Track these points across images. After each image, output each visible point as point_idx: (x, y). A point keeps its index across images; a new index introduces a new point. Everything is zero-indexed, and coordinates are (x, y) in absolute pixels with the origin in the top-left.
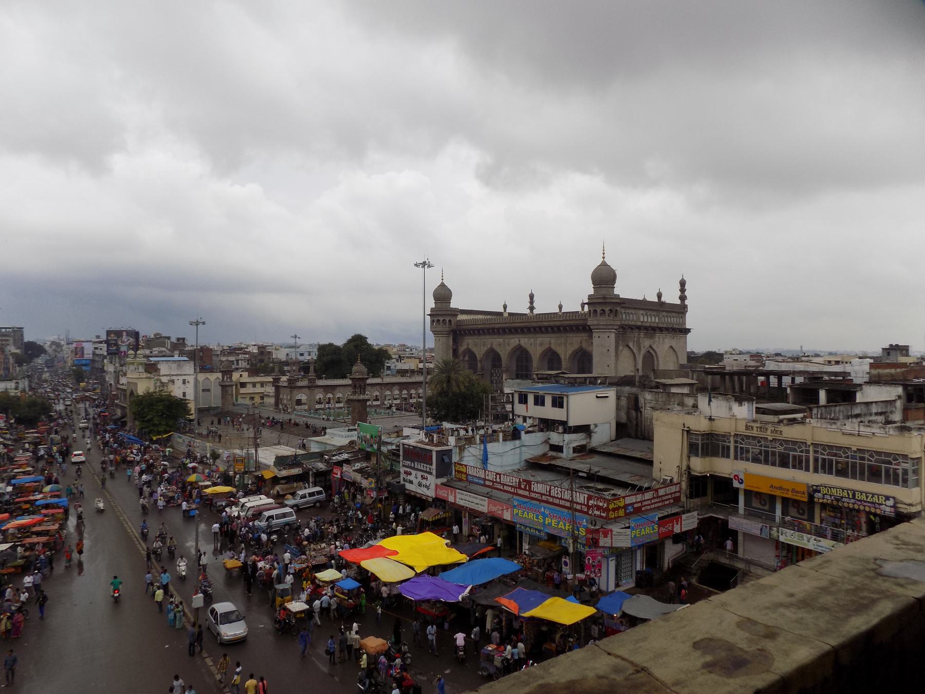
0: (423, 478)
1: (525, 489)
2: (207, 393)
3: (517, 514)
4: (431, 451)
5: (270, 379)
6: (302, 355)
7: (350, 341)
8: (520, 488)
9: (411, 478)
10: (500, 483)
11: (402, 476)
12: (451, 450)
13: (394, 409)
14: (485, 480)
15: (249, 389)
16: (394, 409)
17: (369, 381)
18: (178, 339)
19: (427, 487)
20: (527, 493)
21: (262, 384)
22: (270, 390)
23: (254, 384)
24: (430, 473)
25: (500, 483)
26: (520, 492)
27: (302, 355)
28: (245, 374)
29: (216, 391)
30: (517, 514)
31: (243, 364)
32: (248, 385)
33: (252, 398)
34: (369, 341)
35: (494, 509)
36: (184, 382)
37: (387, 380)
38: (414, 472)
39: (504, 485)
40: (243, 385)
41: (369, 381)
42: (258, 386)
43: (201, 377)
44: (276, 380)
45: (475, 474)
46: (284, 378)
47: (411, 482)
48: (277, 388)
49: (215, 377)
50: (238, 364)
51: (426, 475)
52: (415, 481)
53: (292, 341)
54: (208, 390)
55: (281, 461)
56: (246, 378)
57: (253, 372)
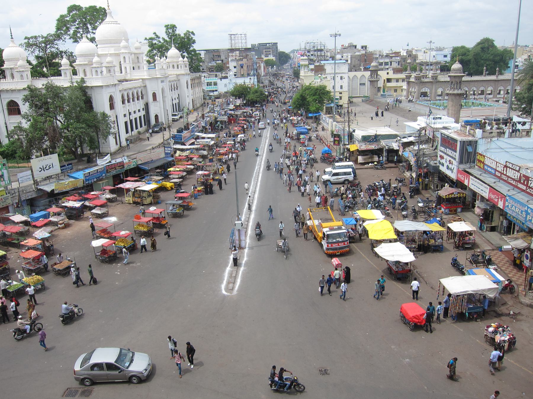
0: (450, 162)
1: (523, 184)
2: (362, 87)
3: (508, 206)
4: (456, 141)
5: (403, 76)
6: (445, 56)
7: (479, 44)
8: (519, 181)
9: (443, 161)
10: (506, 175)
11: (439, 159)
12: (477, 141)
13: (501, 102)
14: (496, 170)
15: (393, 84)
16: (501, 102)
17: (464, 79)
18: (362, 47)
19: (452, 170)
20: (524, 188)
21: (403, 80)
22: (404, 85)
23: (397, 81)
24: (455, 159)
25: (506, 175)
26: (520, 186)
27: (445, 56)
28: (391, 72)
29: (368, 84)
30: (508, 206)
31: (395, 65)
32: (392, 80)
33: (396, 91)
34: (495, 43)
35: (493, 197)
36: (341, 78)
37: (501, 77)
38: (445, 156)
39: (508, 177)
40: (389, 80)
41: (464, 79)
42: (400, 81)
43: (352, 74)
44: (409, 77)
45: (489, 164)
46: (414, 75)
47: (443, 165)
48: (409, 83)
49: (367, 74)
50: (391, 65)
51: (452, 160)
52: (445, 165)
53: (428, 46)
54: (364, 84)
55: (365, 139)
56: (392, 75)
57: (396, 71)
